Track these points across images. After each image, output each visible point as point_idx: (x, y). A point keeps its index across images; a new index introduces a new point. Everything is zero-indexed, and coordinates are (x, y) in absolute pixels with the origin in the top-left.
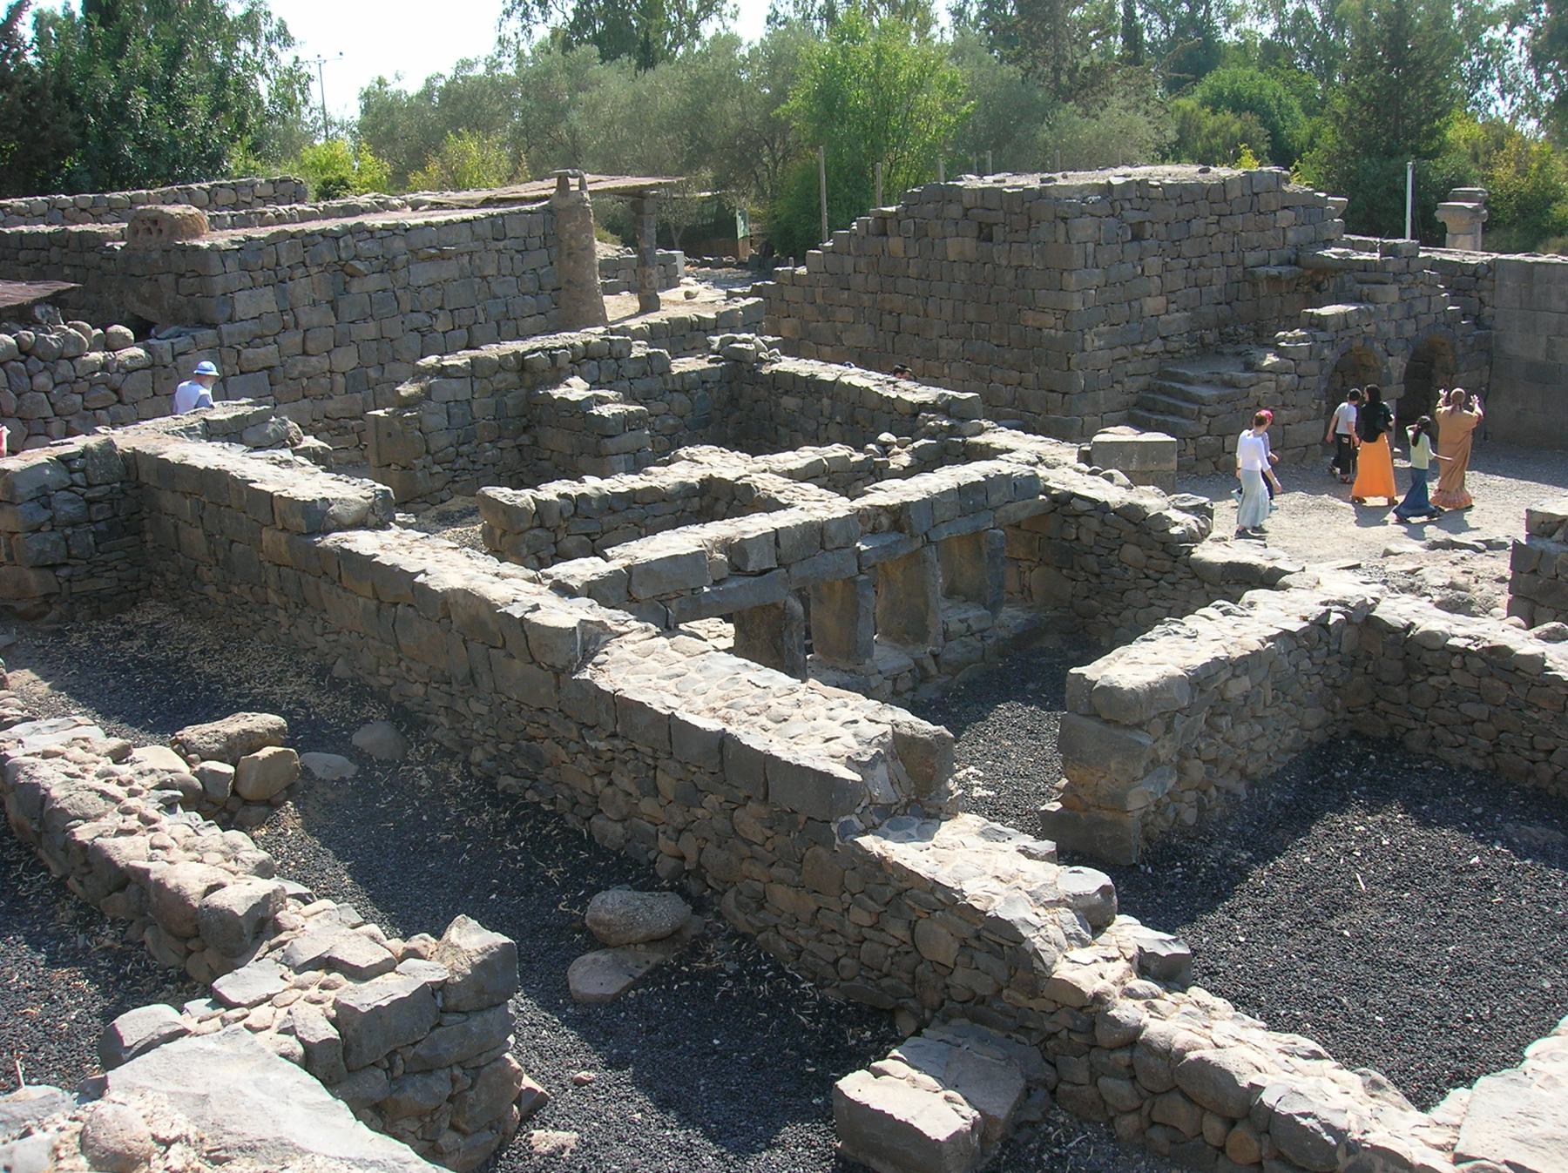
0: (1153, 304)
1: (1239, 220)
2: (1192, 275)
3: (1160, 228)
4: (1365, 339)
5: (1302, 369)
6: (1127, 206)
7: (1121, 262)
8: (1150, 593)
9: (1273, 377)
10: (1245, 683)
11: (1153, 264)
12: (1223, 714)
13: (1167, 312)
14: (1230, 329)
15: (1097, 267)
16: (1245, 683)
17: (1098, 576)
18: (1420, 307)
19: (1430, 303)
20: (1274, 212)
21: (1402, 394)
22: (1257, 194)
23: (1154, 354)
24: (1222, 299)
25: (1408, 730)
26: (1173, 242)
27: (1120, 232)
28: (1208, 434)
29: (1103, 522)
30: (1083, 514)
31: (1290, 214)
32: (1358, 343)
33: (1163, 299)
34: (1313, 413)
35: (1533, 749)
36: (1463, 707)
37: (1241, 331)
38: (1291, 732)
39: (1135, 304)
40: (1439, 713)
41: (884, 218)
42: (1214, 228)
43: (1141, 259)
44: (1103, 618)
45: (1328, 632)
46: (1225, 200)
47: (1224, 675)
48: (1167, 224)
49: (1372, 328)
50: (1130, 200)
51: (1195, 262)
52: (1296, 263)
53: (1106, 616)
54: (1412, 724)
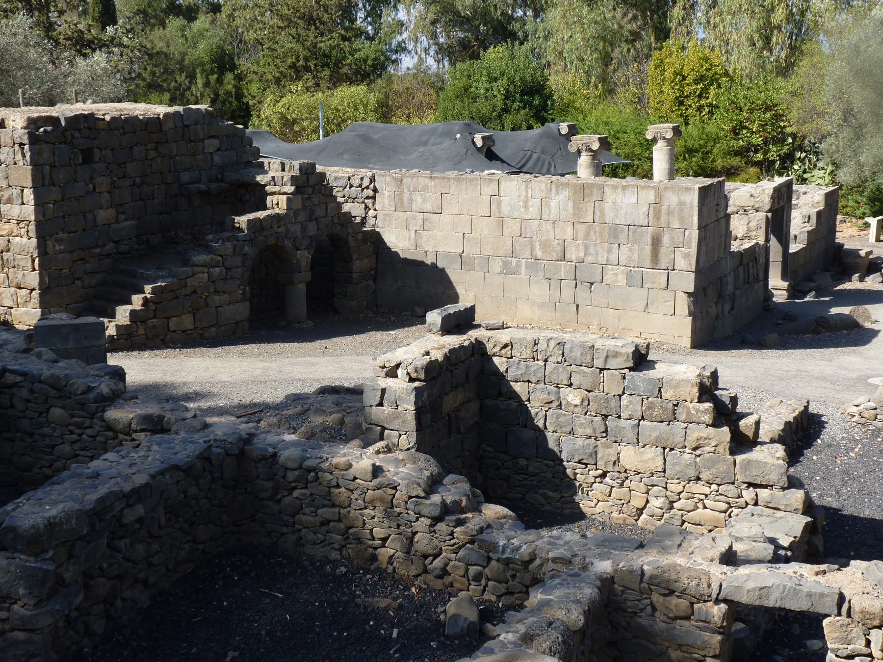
0: (104, 215)
4: (277, 238)
5: (228, 263)
6: (77, 135)
7: (75, 181)
8: (75, 446)
9: (206, 270)
10: (140, 510)
11: (103, 183)
12: (121, 538)
13: (117, 221)
15: (54, 185)
16: (140, 510)
17: (31, 435)
18: (320, 212)
19: (327, 209)
20: (203, 140)
21: (309, 279)
22: (187, 126)
23: (108, 255)
25: (282, 534)
26: (119, 165)
27: (72, 157)
28: (155, 317)
29: (32, 391)
30: (15, 385)
31: (216, 142)
32: (272, 241)
34: (239, 297)
35: (373, 539)
36: (320, 511)
37: (181, 234)
38: (186, 546)
39: (90, 216)
40: (304, 518)
42: (153, 154)
43: (92, 179)
44: (38, 471)
45: (211, 463)
46: (161, 131)
47: (118, 506)
48: (112, 150)
49: (282, 229)
50: (79, 130)
51: (138, 180)
52: (222, 180)
53: (40, 468)
54: (285, 530)
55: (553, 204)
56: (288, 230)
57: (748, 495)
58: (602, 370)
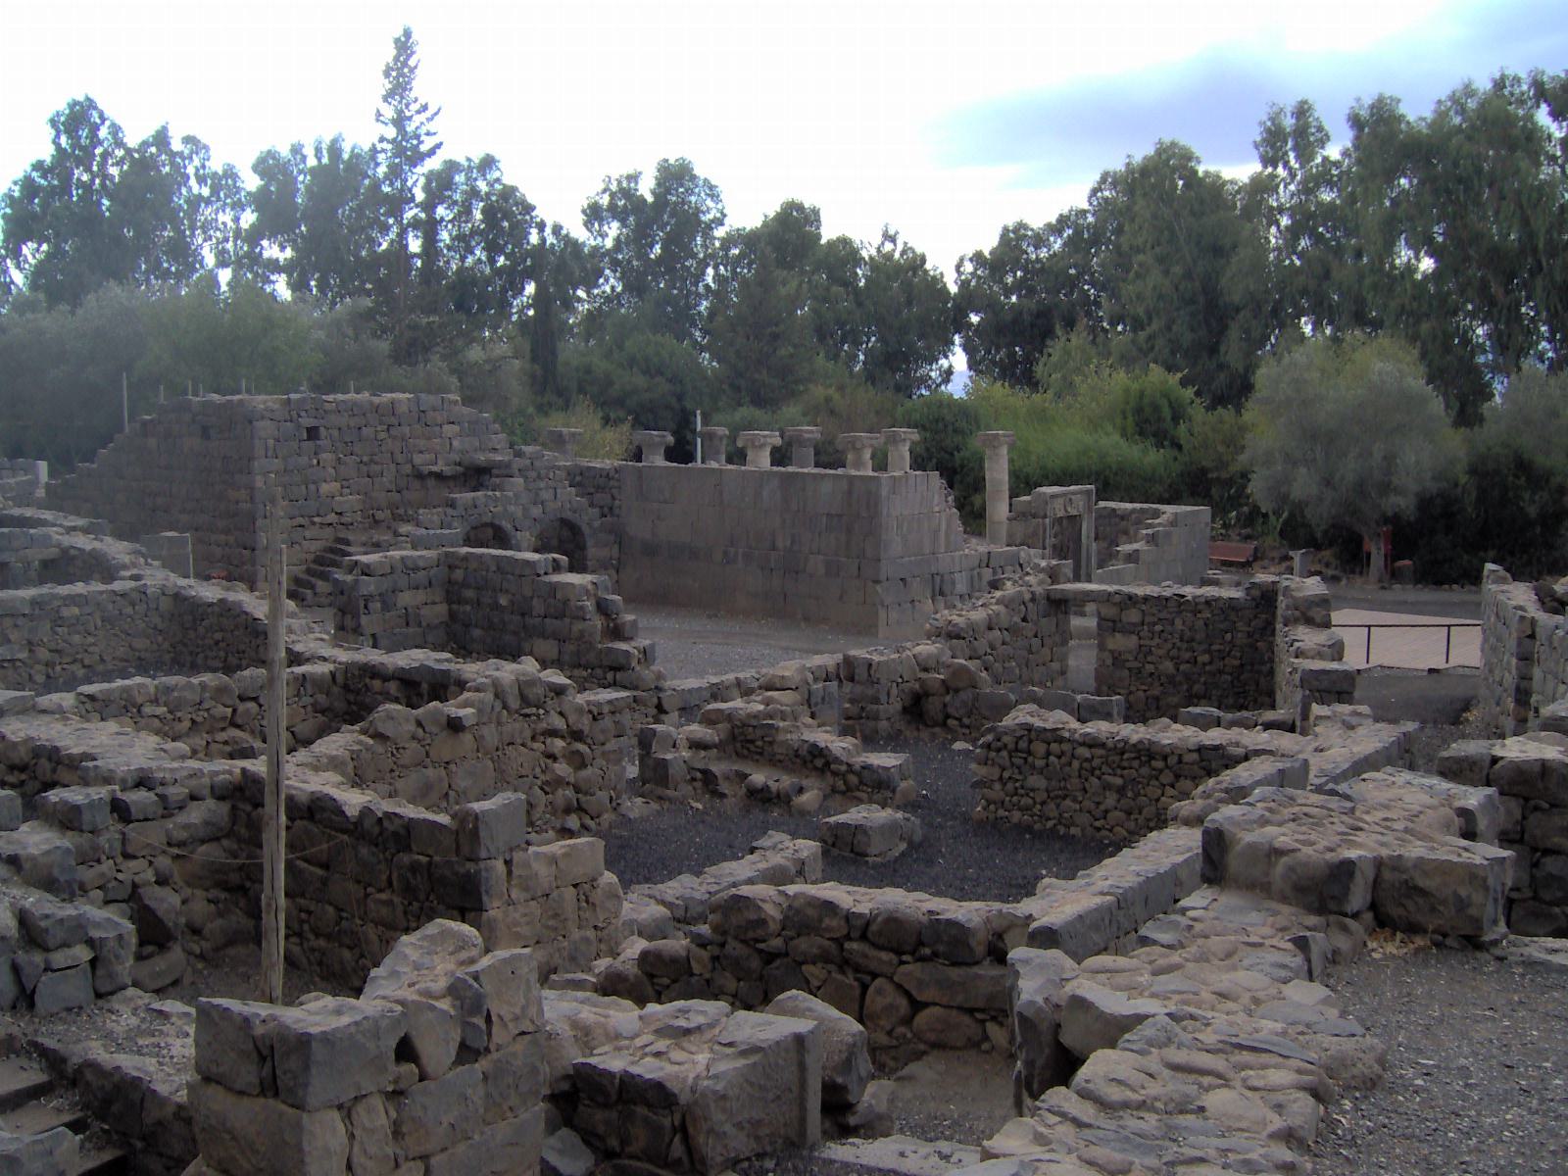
0: (325, 488)
1: (406, 430)
2: (364, 469)
3: (335, 433)
6: (303, 414)
14: (401, 511)
24: (393, 488)
31: (456, 428)
32: (487, 519)
33: (338, 485)
39: (312, 487)
41: (145, 424)
42: (383, 435)
47: (56, 603)
49: (500, 509)
55: (765, 493)
56: (506, 510)
57: (610, 676)
58: (520, 576)
